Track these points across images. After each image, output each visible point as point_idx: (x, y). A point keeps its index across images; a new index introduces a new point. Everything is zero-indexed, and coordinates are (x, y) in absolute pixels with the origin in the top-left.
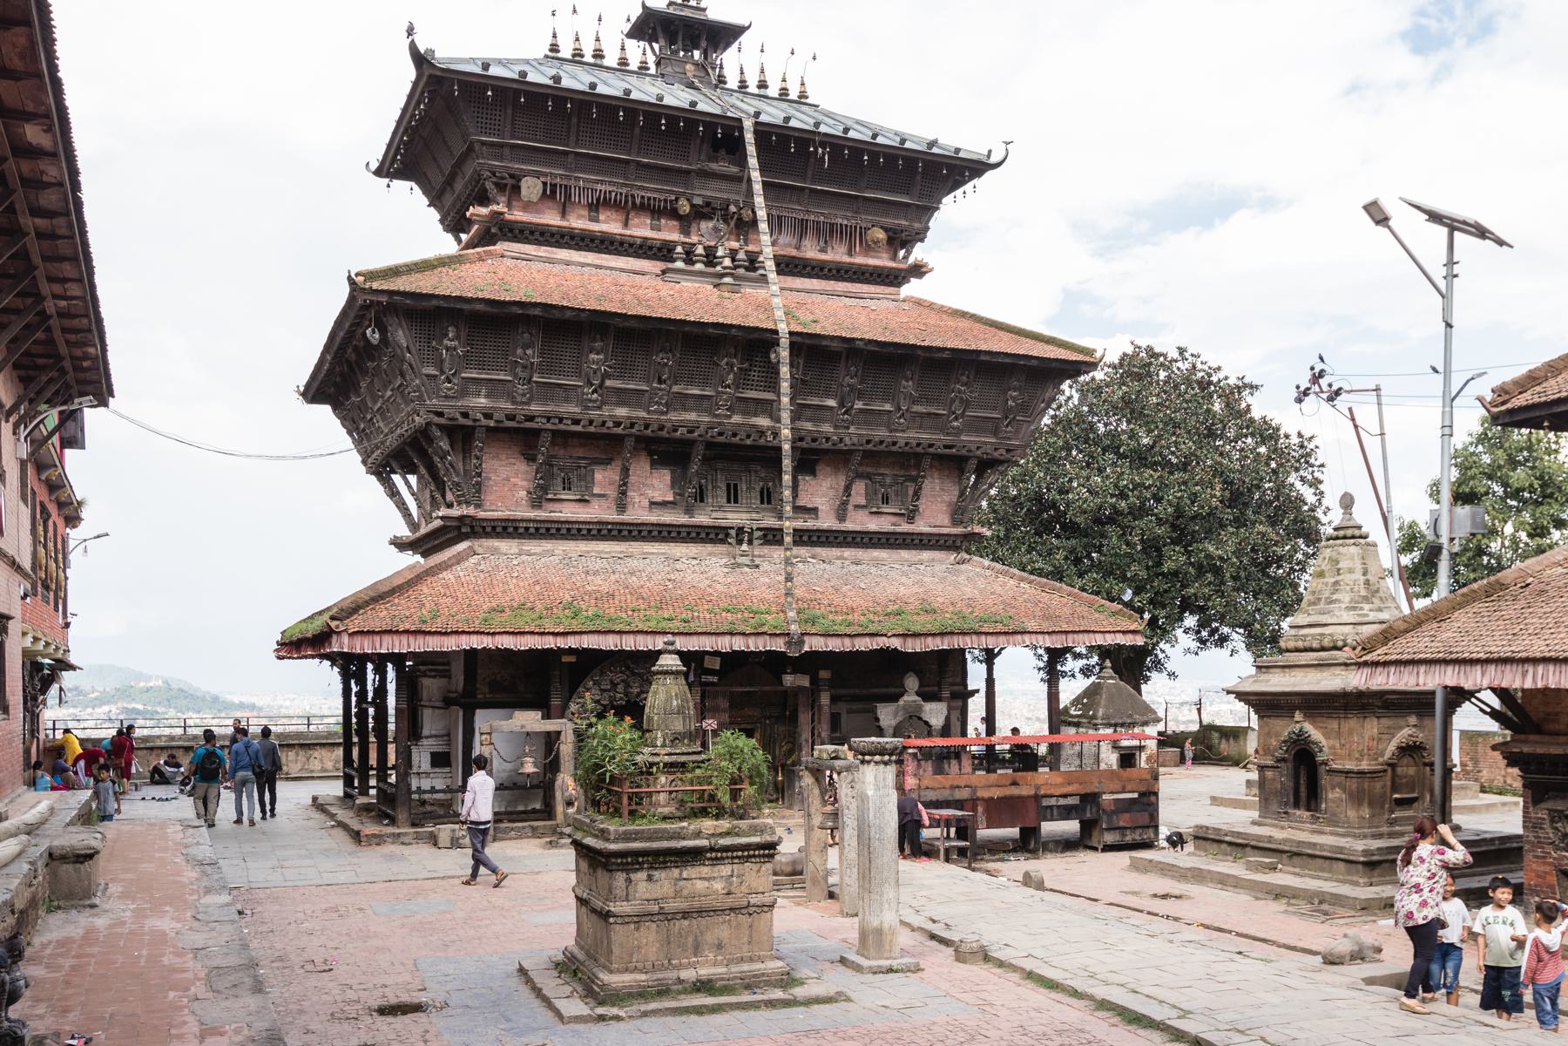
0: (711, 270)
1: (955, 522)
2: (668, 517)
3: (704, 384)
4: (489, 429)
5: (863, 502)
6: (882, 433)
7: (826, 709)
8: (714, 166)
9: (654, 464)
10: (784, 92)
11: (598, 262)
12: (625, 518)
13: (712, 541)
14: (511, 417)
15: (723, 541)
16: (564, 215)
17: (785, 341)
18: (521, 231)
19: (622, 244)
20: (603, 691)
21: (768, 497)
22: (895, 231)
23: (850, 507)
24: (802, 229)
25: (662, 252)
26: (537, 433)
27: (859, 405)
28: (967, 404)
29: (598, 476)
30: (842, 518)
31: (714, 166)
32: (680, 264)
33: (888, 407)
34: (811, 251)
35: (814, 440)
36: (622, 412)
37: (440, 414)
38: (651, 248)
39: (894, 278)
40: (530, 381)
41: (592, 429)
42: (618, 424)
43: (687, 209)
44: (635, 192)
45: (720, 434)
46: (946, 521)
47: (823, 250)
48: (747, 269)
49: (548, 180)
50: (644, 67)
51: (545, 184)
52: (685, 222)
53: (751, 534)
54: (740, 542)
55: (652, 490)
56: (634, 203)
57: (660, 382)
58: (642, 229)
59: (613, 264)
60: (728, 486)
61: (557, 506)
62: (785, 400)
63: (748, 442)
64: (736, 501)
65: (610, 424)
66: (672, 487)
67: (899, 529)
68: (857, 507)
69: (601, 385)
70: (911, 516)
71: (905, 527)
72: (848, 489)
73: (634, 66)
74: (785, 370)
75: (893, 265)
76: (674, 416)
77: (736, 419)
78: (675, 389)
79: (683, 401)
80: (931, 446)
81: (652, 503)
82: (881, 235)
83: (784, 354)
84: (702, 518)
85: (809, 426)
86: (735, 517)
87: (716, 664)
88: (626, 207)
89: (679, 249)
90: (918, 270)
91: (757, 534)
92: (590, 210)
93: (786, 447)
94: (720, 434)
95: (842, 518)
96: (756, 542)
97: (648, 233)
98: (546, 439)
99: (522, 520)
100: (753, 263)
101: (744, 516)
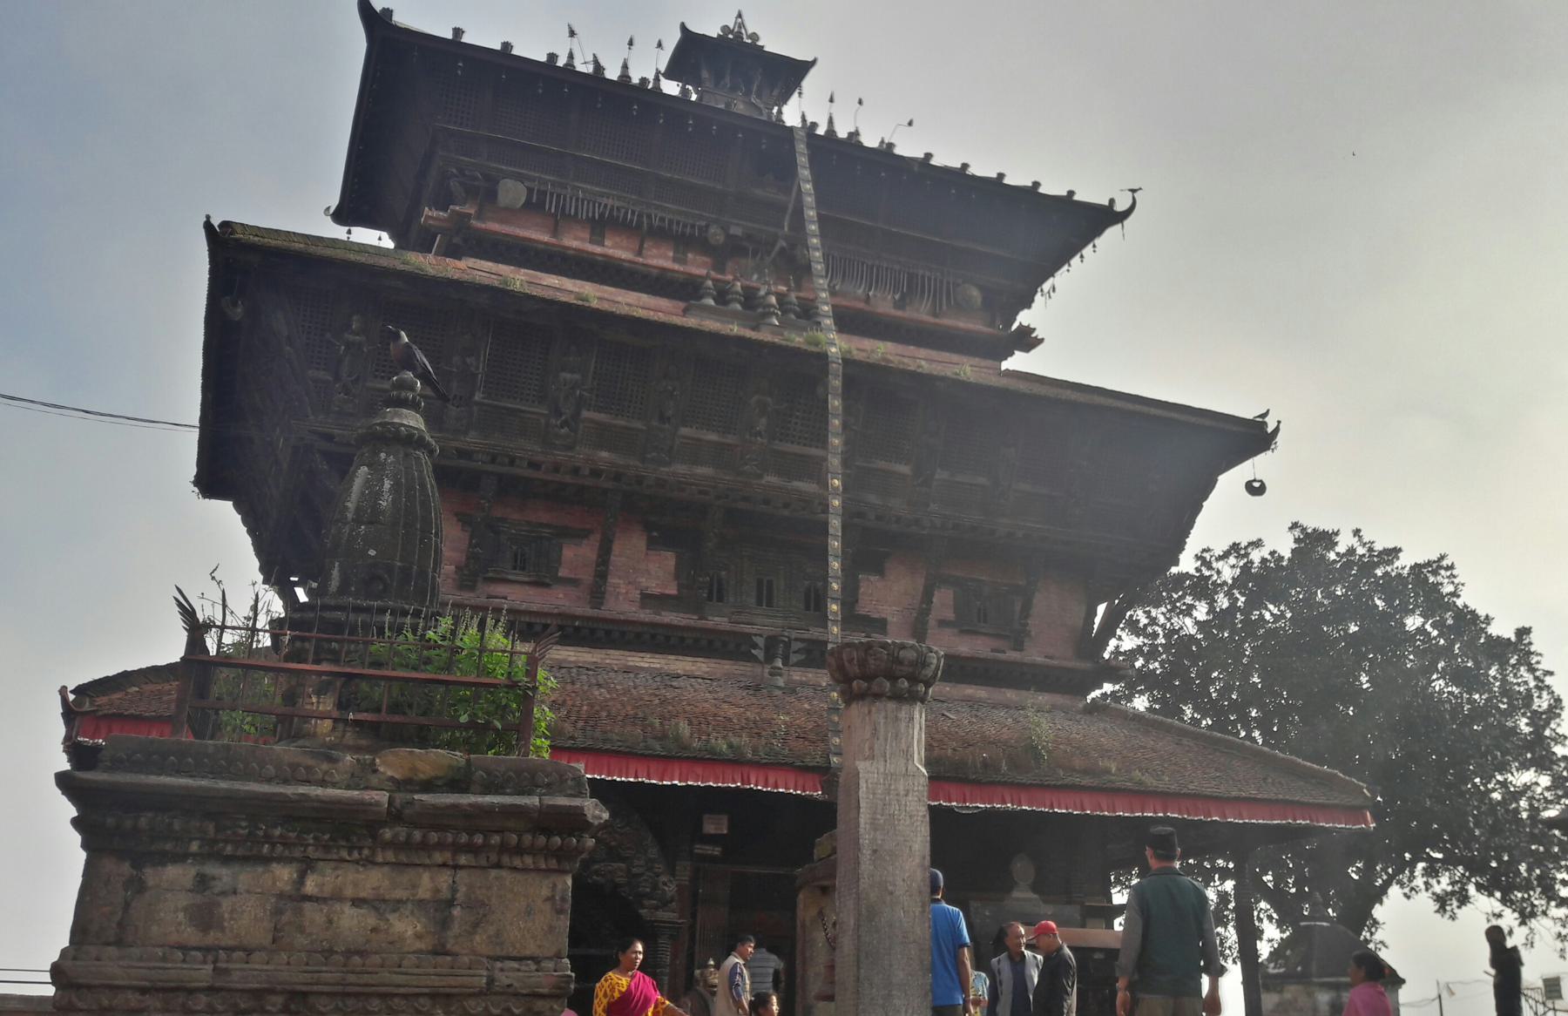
2: (670, 617)
5: (950, 615)
8: (759, 192)
9: (652, 544)
12: (603, 613)
17: (836, 367)
21: (815, 602)
23: (932, 621)
27: (941, 475)
29: (569, 553)
31: (759, 192)
33: (982, 480)
34: (884, 305)
35: (879, 518)
41: (558, 477)
43: (721, 238)
44: (653, 212)
45: (746, 499)
48: (798, 316)
49: (535, 186)
51: (530, 191)
53: (788, 645)
54: (770, 658)
55: (642, 574)
56: (650, 226)
57: (663, 418)
58: (660, 258)
60: (760, 583)
63: (786, 513)
64: (769, 604)
65: (587, 472)
66: (677, 577)
68: (943, 623)
70: (1019, 646)
72: (927, 596)
74: (835, 403)
76: (681, 468)
78: (684, 431)
81: (647, 599)
83: (836, 383)
84: (718, 621)
90: (1026, 339)
91: (799, 645)
92: (592, 233)
93: (836, 503)
94: (746, 499)
96: (794, 658)
97: (668, 264)
100: (808, 312)
101: (780, 622)
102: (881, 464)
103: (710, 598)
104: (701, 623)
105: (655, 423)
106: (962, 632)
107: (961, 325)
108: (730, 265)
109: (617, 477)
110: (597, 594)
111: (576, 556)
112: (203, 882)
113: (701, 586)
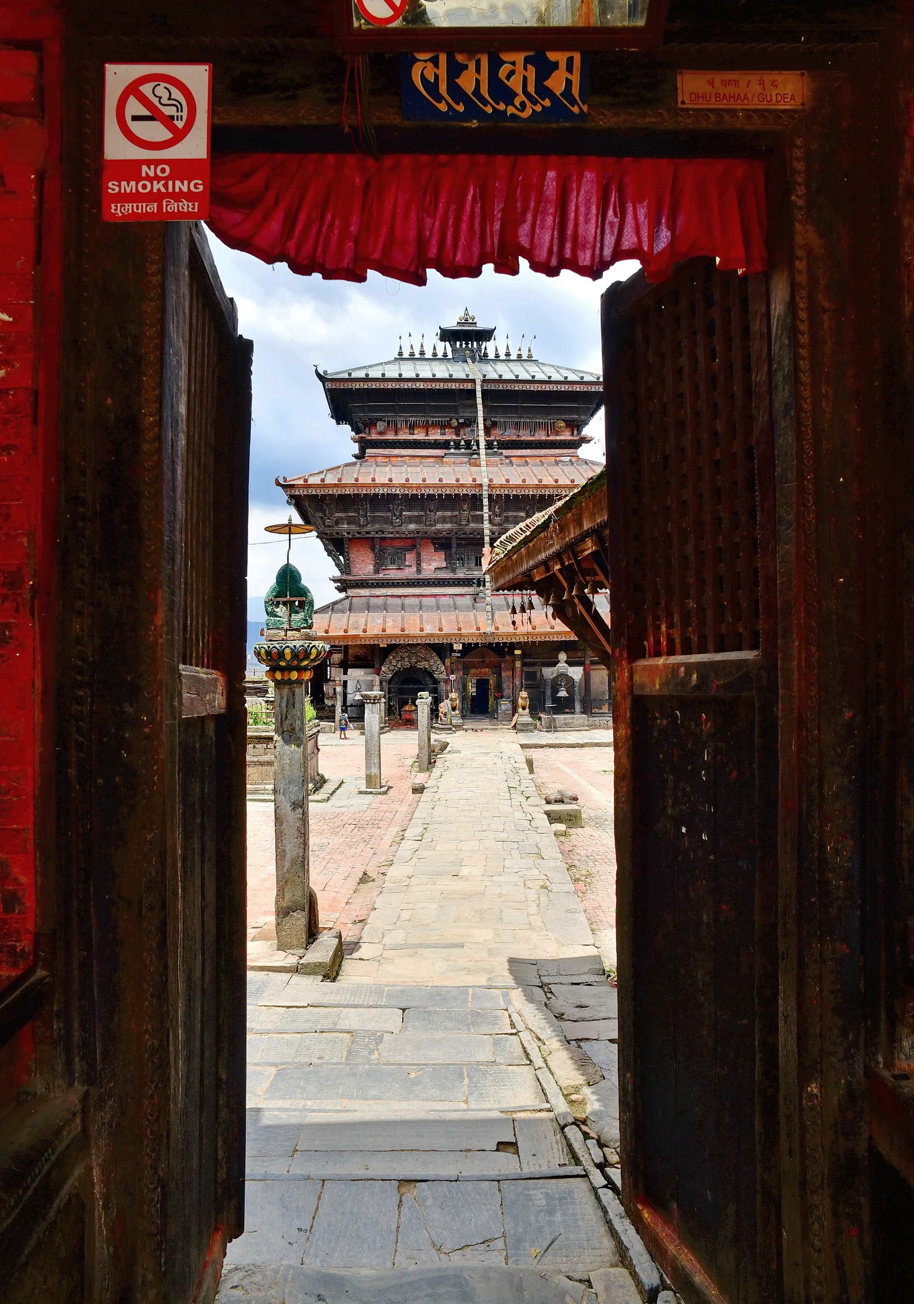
0: (469, 451)
3: (453, 510)
4: (350, 539)
10: (519, 356)
12: (421, 576)
13: (466, 586)
14: (359, 533)
16: (396, 433)
18: (375, 443)
19: (425, 443)
22: (571, 421)
24: (517, 426)
25: (445, 445)
26: (373, 538)
29: (408, 556)
31: (468, 402)
34: (526, 436)
36: (412, 526)
37: (326, 534)
38: (440, 444)
39: (575, 445)
43: (456, 424)
50: (445, 355)
54: (479, 586)
58: (436, 435)
59: (421, 454)
61: (388, 572)
62: (486, 516)
66: (446, 560)
69: (401, 515)
73: (440, 356)
75: (571, 438)
76: (439, 526)
79: (444, 520)
82: (563, 424)
84: (461, 574)
86: (477, 574)
87: (458, 647)
88: (427, 427)
89: (452, 443)
97: (438, 437)
98: (377, 542)
102: (514, 514)
104: (456, 576)
107: (558, 438)
108: (462, 433)
109: (418, 533)
110: (419, 571)
111: (410, 557)
112: (254, 747)
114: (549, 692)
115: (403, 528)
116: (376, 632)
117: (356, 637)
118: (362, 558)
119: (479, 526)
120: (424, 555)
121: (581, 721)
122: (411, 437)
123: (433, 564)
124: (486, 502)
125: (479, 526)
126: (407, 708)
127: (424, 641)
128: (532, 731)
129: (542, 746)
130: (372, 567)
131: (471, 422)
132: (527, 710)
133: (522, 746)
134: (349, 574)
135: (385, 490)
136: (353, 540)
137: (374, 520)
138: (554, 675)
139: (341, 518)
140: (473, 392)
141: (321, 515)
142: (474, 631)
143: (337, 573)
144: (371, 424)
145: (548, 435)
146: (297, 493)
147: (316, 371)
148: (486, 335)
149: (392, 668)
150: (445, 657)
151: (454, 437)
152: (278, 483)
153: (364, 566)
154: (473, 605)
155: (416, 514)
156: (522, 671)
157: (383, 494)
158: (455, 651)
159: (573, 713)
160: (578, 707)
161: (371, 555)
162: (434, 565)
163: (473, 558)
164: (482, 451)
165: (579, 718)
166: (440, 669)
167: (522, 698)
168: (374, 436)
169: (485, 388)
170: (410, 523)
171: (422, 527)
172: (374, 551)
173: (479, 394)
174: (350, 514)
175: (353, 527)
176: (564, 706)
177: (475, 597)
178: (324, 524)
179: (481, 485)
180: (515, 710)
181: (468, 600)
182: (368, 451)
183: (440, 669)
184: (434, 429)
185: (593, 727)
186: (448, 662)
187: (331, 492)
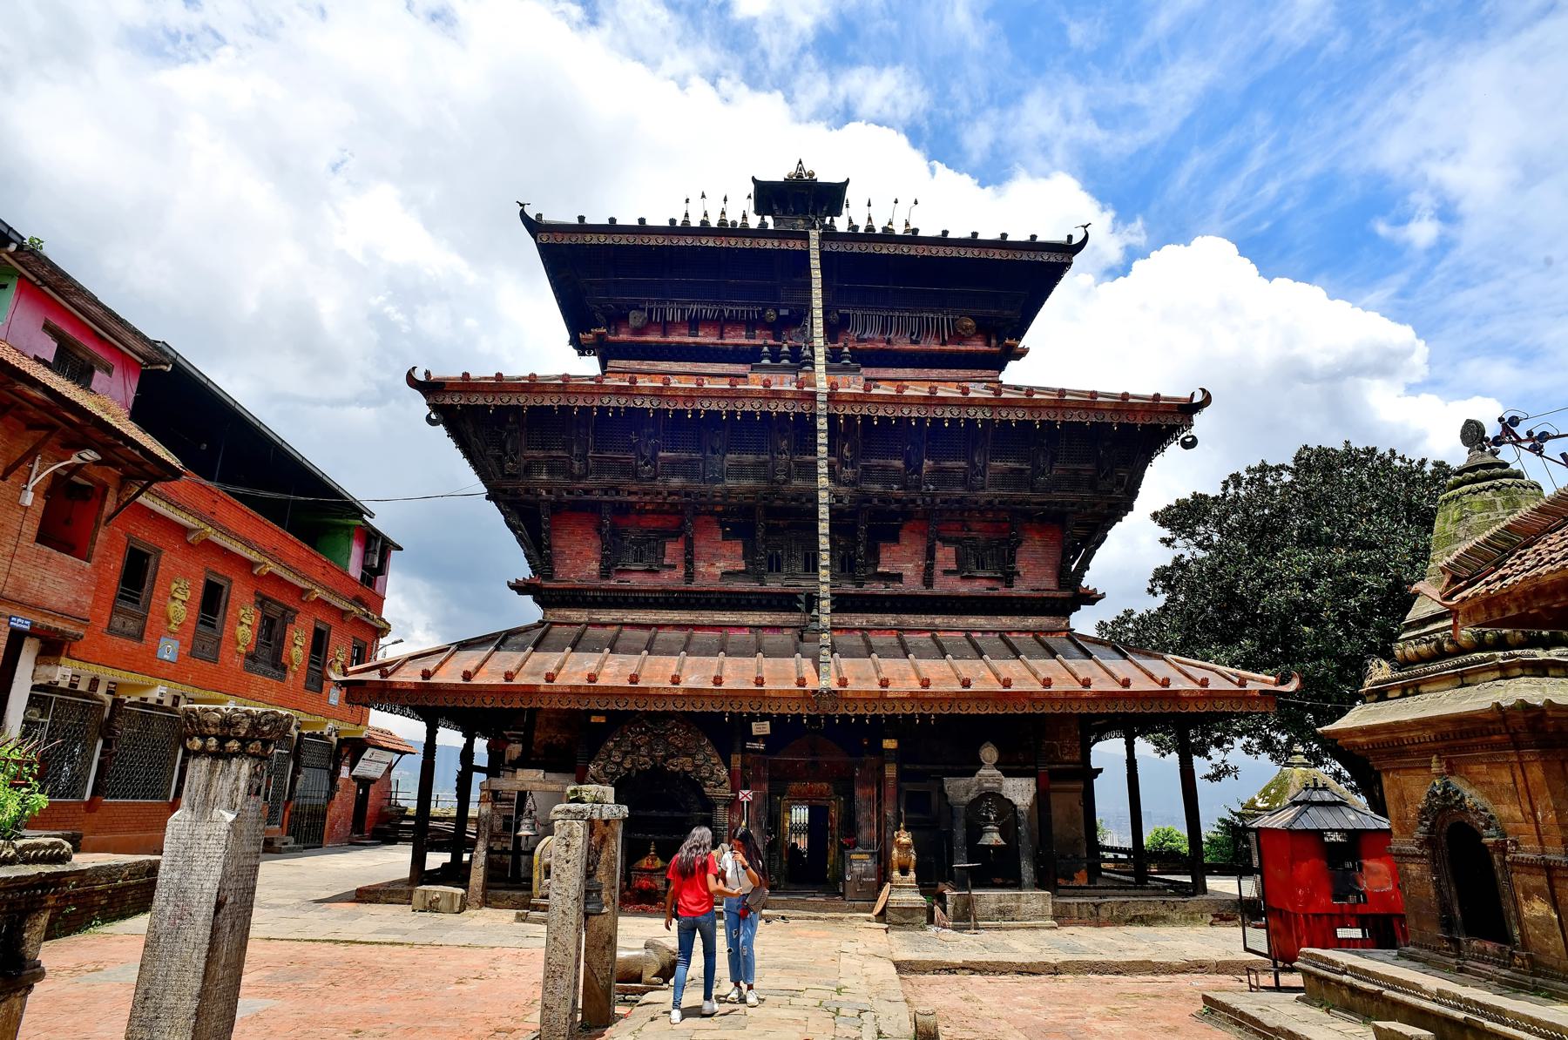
1: (1061, 587)
3: (759, 451)
4: (552, 503)
5: (954, 567)
6: (959, 491)
7: (891, 783)
9: (726, 537)
11: (695, 370)
12: (693, 586)
15: (793, 609)
16: (665, 334)
20: (627, 753)
23: (938, 570)
27: (928, 463)
28: (1054, 459)
30: (928, 581)
31: (799, 280)
32: (766, 361)
33: (963, 464)
34: (903, 344)
36: (676, 482)
37: (505, 491)
38: (744, 352)
40: (583, 457)
42: (670, 494)
43: (774, 318)
46: (1053, 585)
47: (913, 342)
52: (778, 328)
54: (809, 610)
59: (709, 371)
61: (626, 577)
66: (745, 557)
67: (996, 593)
68: (947, 572)
69: (654, 457)
70: (1009, 578)
71: (1002, 591)
72: (930, 554)
76: (731, 483)
77: (797, 483)
79: (740, 471)
80: (1020, 503)
84: (774, 585)
85: (877, 488)
87: (761, 728)
88: (721, 324)
95: (928, 581)
99: (588, 590)
103: (770, 570)
104: (764, 588)
105: (708, 454)
106: (963, 578)
107: (962, 348)
109: (687, 494)
110: (690, 576)
111: (673, 550)
113: (762, 560)
114: (960, 834)
115: (659, 483)
116: (575, 682)
117: (530, 691)
118: (577, 548)
119: (810, 485)
120: (701, 546)
121: (1036, 905)
122: (691, 340)
123: (719, 564)
124: (822, 424)
125: (810, 485)
126: (644, 863)
127: (679, 707)
128: (922, 928)
129: (951, 969)
130: (595, 566)
131: (800, 317)
132: (912, 875)
133: (902, 967)
134: (550, 578)
135: (623, 401)
136: (557, 508)
137: (602, 467)
138: (972, 795)
139: (537, 461)
140: (805, 255)
141: (497, 452)
142: (793, 686)
143: (524, 572)
144: (617, 319)
145: (944, 343)
146: (448, 401)
147: (523, 214)
148: (832, 197)
149: (611, 768)
150: (732, 751)
151: (771, 342)
152: (411, 381)
153: (581, 563)
154: (796, 644)
155: (685, 455)
156: (899, 790)
157: (617, 409)
158: (756, 739)
159: (1017, 884)
160: (1027, 870)
161: (596, 543)
162: (721, 566)
163: (800, 555)
164: (820, 359)
165: (1035, 900)
166: (717, 777)
167: (900, 846)
168: (624, 337)
169: (827, 249)
170: (673, 475)
171: (696, 485)
172: (599, 531)
173: (815, 256)
174: (554, 453)
175: (559, 479)
176: (998, 870)
177: (802, 632)
178: (502, 469)
179: (814, 395)
180: (883, 876)
181: (787, 637)
182: (611, 363)
183: (717, 777)
184: (734, 329)
185: (1062, 917)
186: (737, 761)
187: (514, 402)
